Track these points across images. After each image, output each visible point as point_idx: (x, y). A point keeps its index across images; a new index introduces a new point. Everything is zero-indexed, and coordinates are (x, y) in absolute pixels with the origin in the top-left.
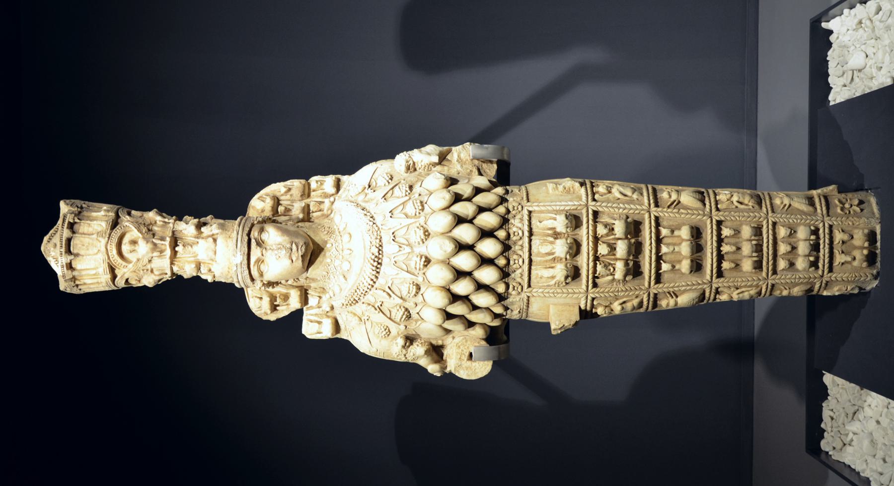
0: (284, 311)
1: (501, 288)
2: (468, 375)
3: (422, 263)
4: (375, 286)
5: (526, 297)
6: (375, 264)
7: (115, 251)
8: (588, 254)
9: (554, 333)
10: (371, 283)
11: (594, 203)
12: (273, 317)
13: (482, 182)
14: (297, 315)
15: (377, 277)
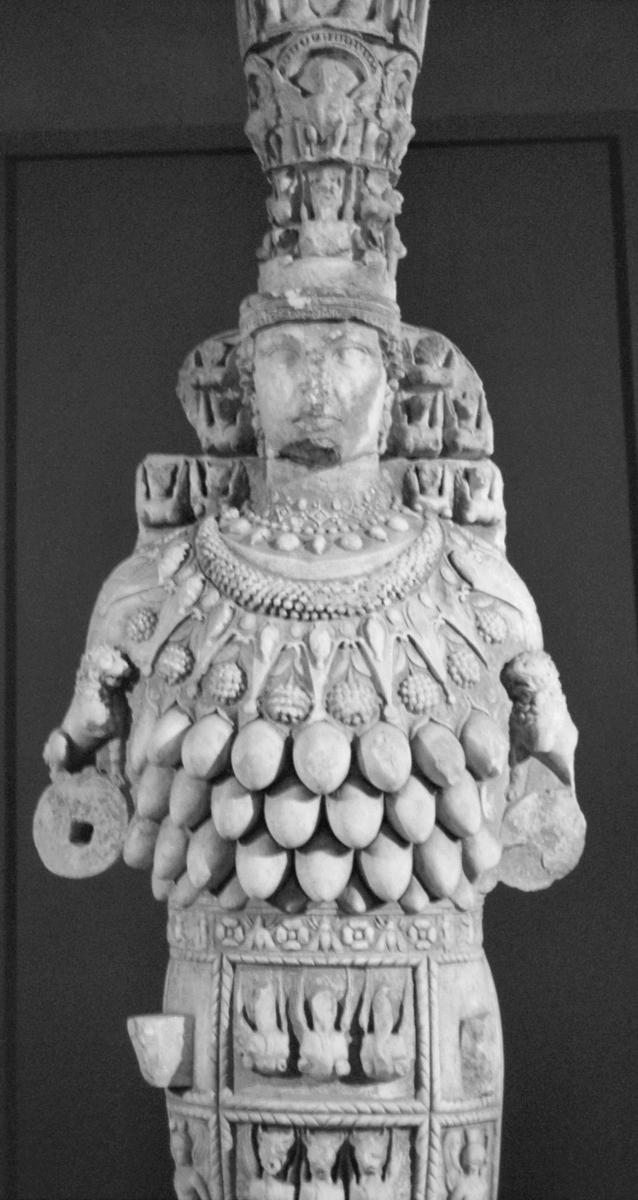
0: (196, 416)
1: (228, 898)
2: (40, 822)
3: (285, 710)
4: (240, 610)
5: (211, 957)
6: (288, 605)
7: (313, 44)
8: (311, 1113)
9: (130, 1023)
10: (246, 596)
11: (437, 1128)
12: (184, 390)
13: (488, 853)
14: (184, 441)
15: (256, 609)
